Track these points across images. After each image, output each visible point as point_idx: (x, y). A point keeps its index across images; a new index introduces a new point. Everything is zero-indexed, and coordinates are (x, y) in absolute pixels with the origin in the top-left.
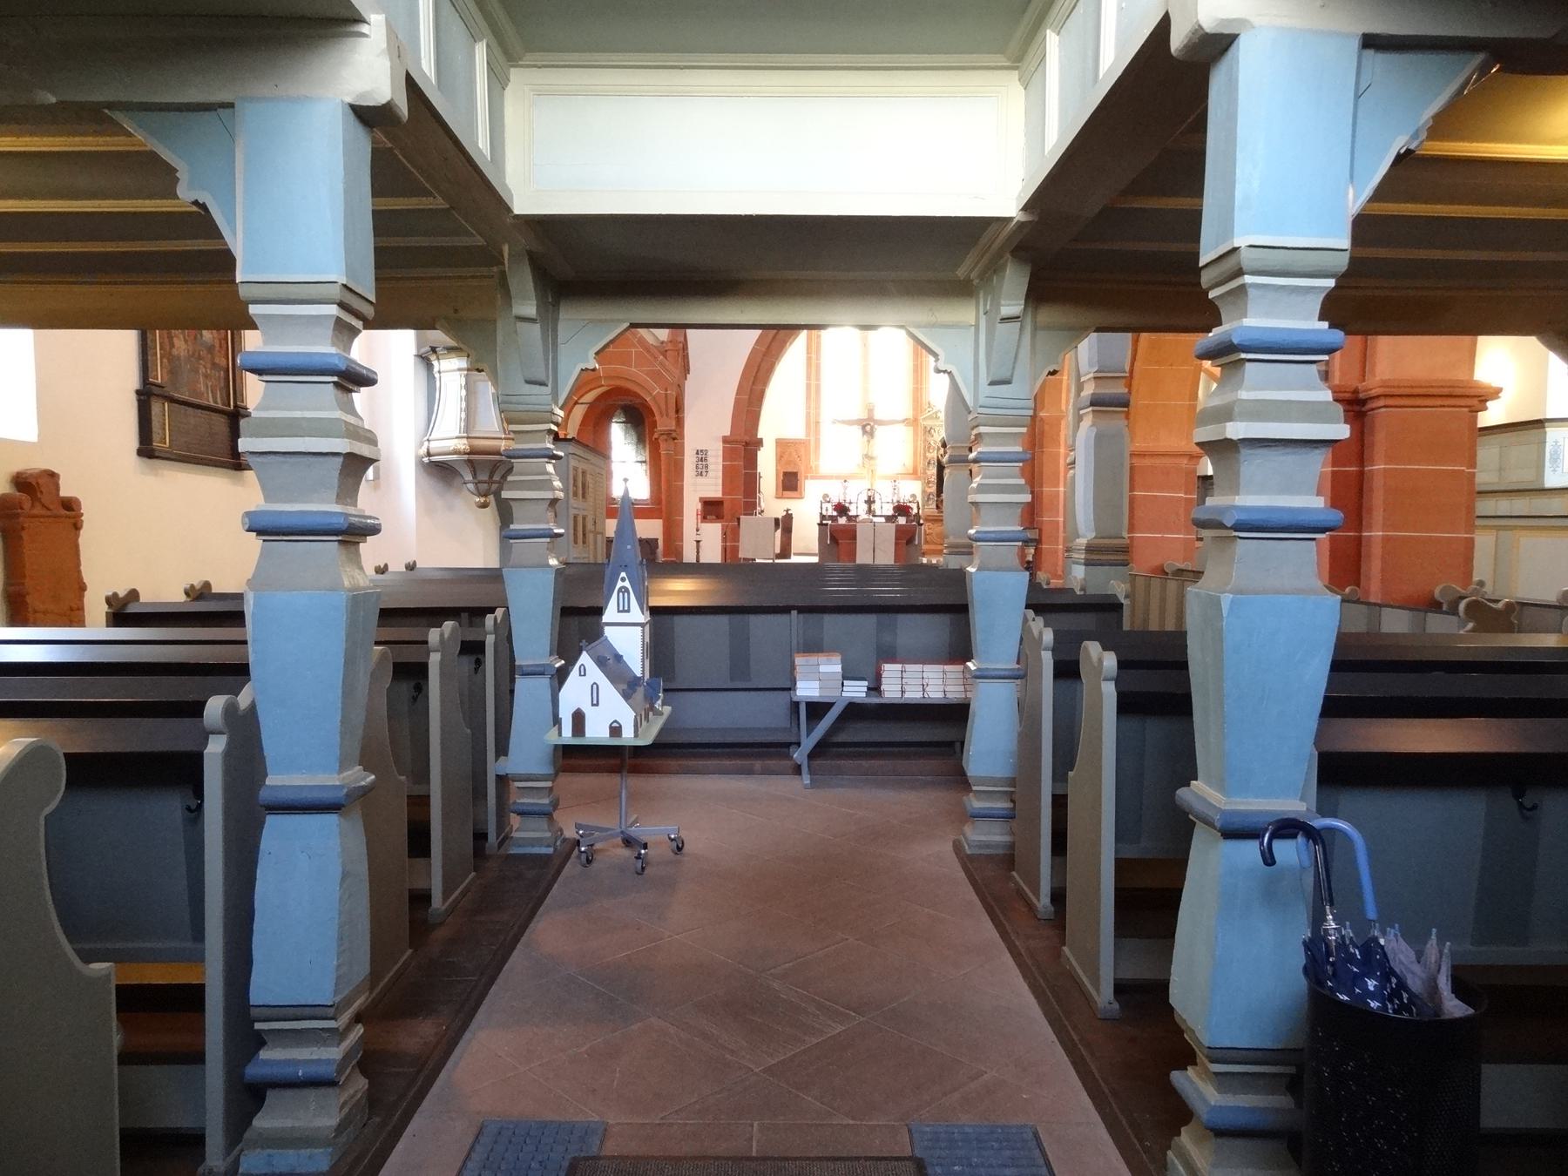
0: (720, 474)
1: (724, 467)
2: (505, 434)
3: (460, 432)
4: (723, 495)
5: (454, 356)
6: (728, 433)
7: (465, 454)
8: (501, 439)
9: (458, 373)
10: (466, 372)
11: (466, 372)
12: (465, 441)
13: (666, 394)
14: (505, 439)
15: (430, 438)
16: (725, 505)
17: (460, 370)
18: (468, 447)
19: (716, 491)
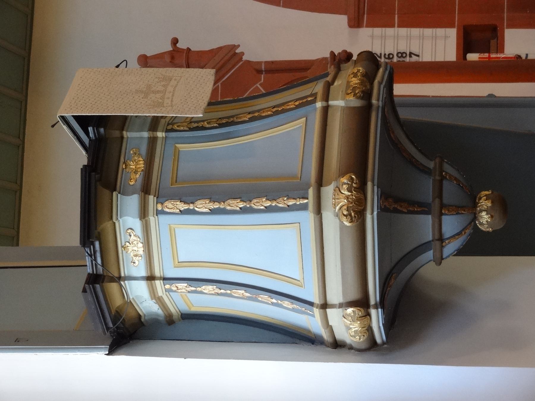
0: (415, 31)
1: (401, 25)
2: (314, 101)
3: (304, 207)
4: (452, 26)
5: (107, 225)
6: (343, 19)
7: (362, 188)
8: (326, 110)
9: (152, 219)
10: (151, 199)
11: (151, 199)
12: (328, 191)
13: (268, 71)
14: (326, 97)
15: (316, 299)
16: (474, 20)
17: (143, 214)
18: (344, 180)
19: (446, 37)
